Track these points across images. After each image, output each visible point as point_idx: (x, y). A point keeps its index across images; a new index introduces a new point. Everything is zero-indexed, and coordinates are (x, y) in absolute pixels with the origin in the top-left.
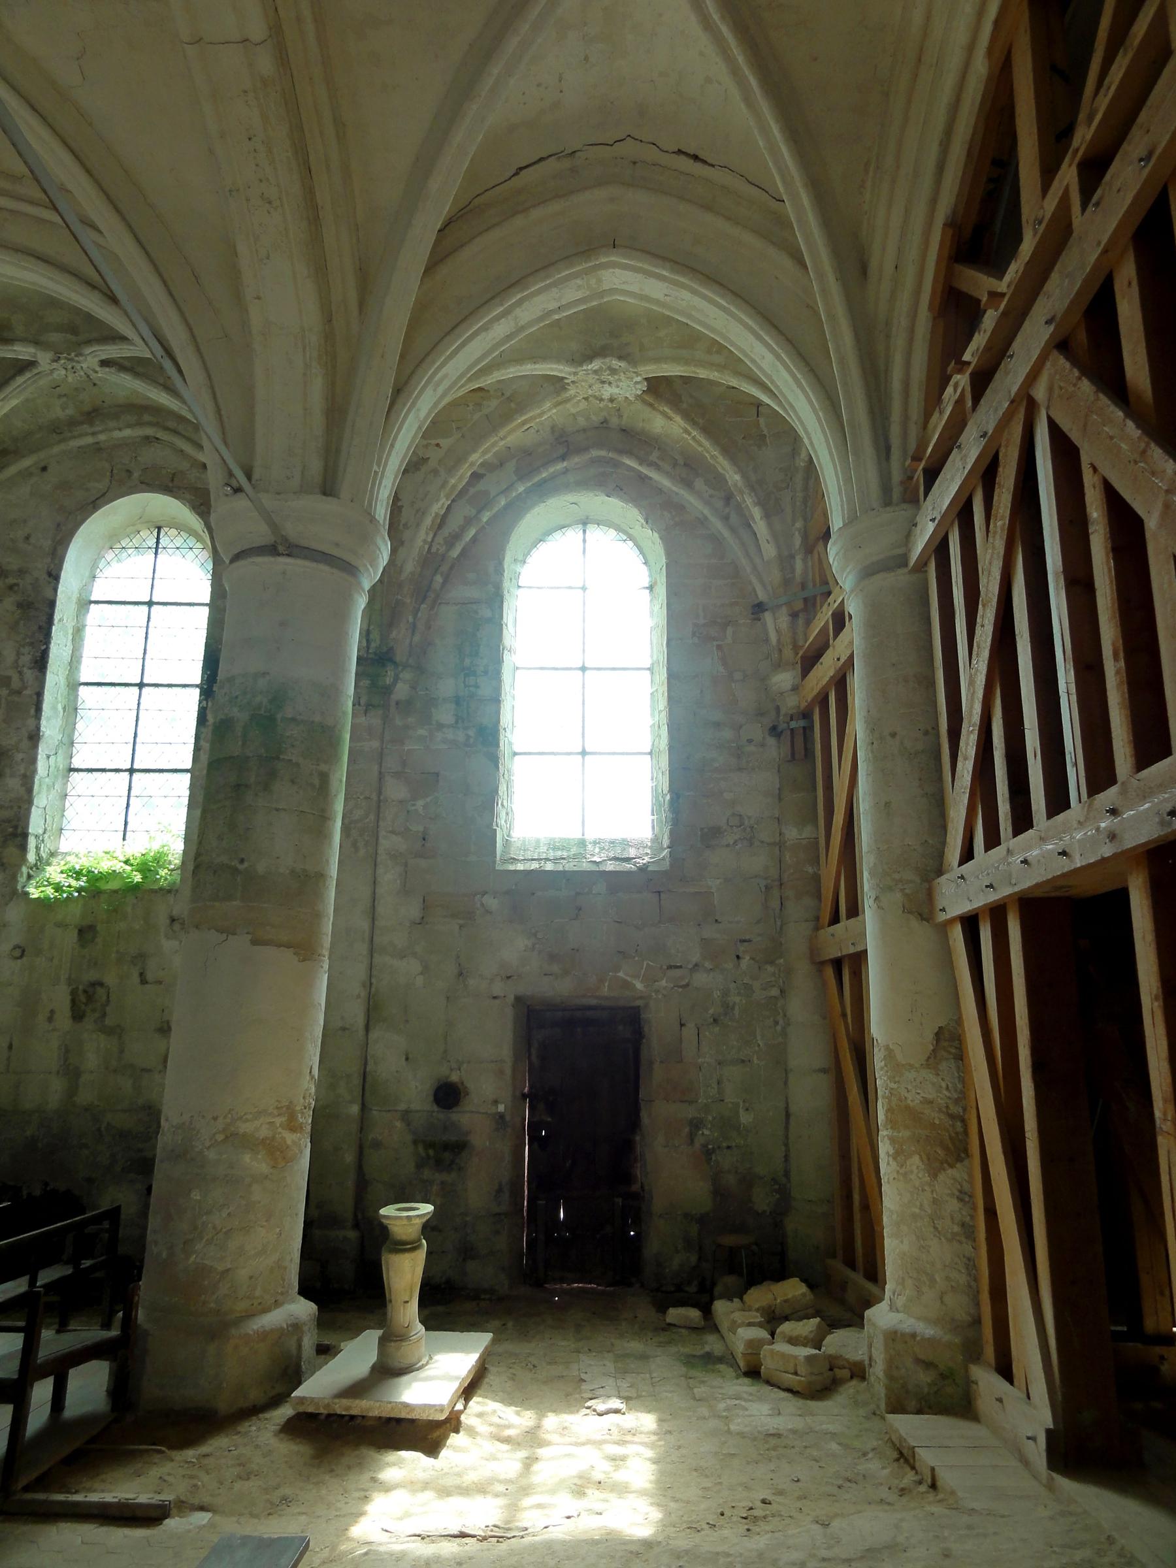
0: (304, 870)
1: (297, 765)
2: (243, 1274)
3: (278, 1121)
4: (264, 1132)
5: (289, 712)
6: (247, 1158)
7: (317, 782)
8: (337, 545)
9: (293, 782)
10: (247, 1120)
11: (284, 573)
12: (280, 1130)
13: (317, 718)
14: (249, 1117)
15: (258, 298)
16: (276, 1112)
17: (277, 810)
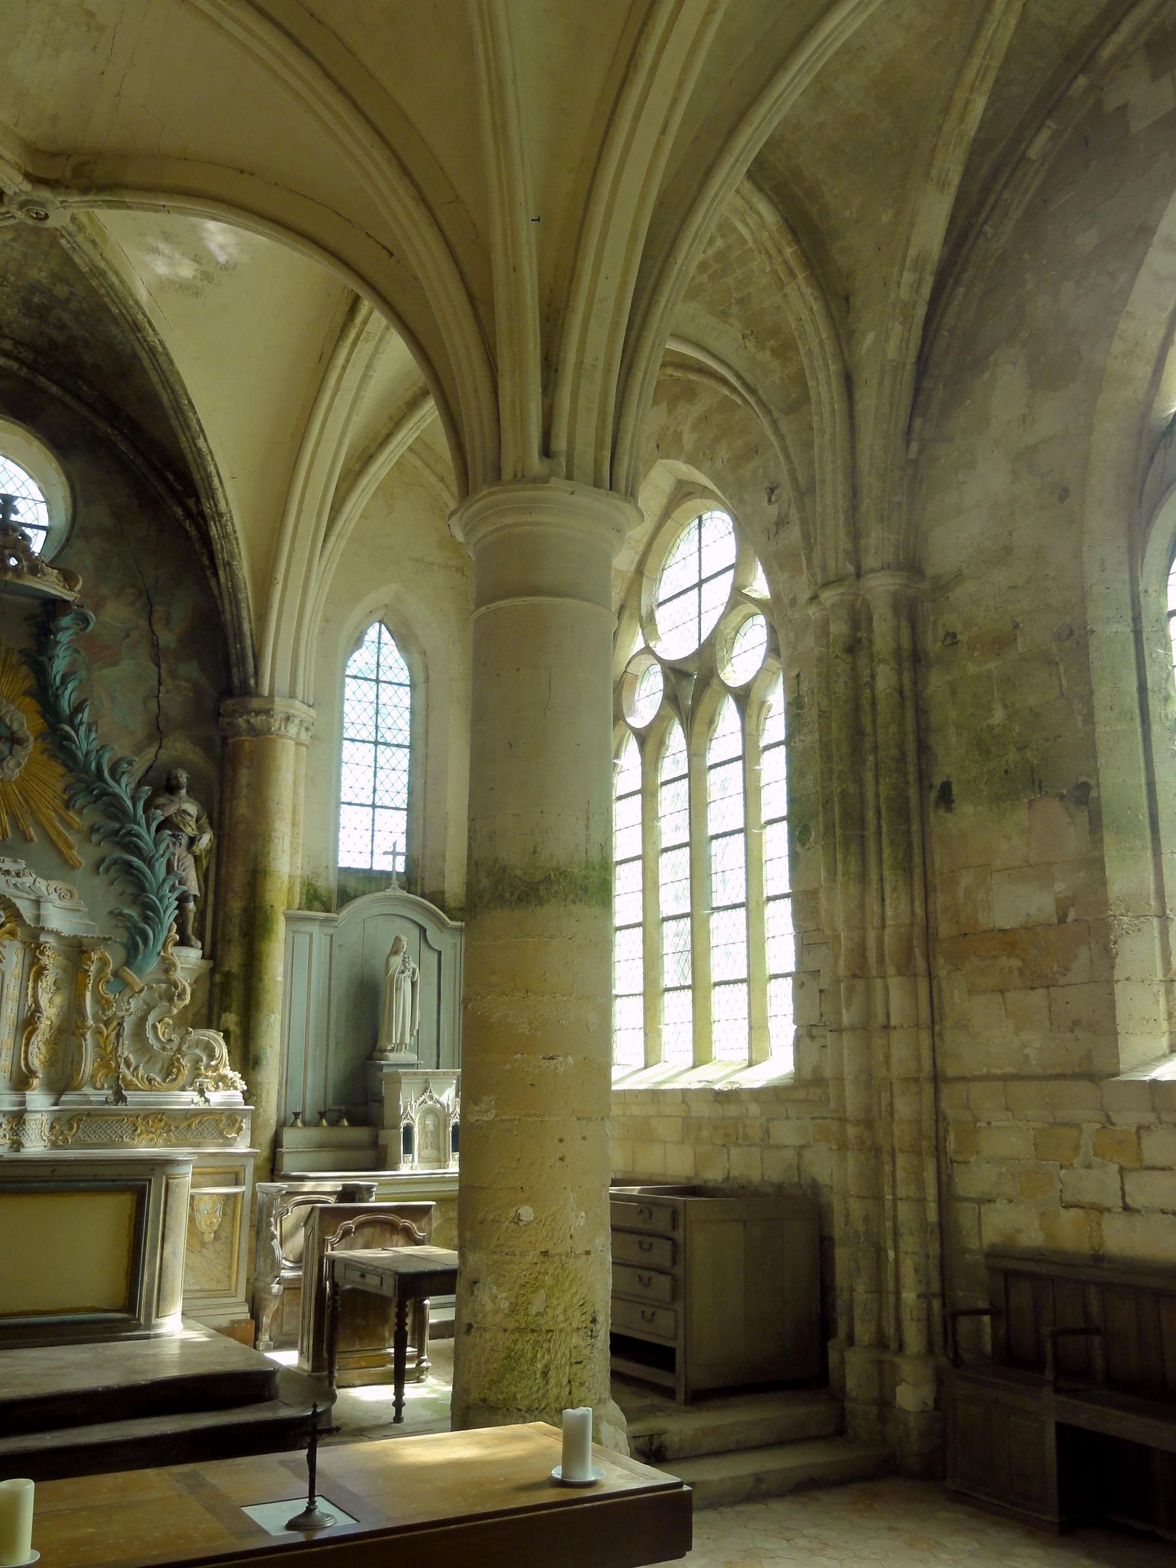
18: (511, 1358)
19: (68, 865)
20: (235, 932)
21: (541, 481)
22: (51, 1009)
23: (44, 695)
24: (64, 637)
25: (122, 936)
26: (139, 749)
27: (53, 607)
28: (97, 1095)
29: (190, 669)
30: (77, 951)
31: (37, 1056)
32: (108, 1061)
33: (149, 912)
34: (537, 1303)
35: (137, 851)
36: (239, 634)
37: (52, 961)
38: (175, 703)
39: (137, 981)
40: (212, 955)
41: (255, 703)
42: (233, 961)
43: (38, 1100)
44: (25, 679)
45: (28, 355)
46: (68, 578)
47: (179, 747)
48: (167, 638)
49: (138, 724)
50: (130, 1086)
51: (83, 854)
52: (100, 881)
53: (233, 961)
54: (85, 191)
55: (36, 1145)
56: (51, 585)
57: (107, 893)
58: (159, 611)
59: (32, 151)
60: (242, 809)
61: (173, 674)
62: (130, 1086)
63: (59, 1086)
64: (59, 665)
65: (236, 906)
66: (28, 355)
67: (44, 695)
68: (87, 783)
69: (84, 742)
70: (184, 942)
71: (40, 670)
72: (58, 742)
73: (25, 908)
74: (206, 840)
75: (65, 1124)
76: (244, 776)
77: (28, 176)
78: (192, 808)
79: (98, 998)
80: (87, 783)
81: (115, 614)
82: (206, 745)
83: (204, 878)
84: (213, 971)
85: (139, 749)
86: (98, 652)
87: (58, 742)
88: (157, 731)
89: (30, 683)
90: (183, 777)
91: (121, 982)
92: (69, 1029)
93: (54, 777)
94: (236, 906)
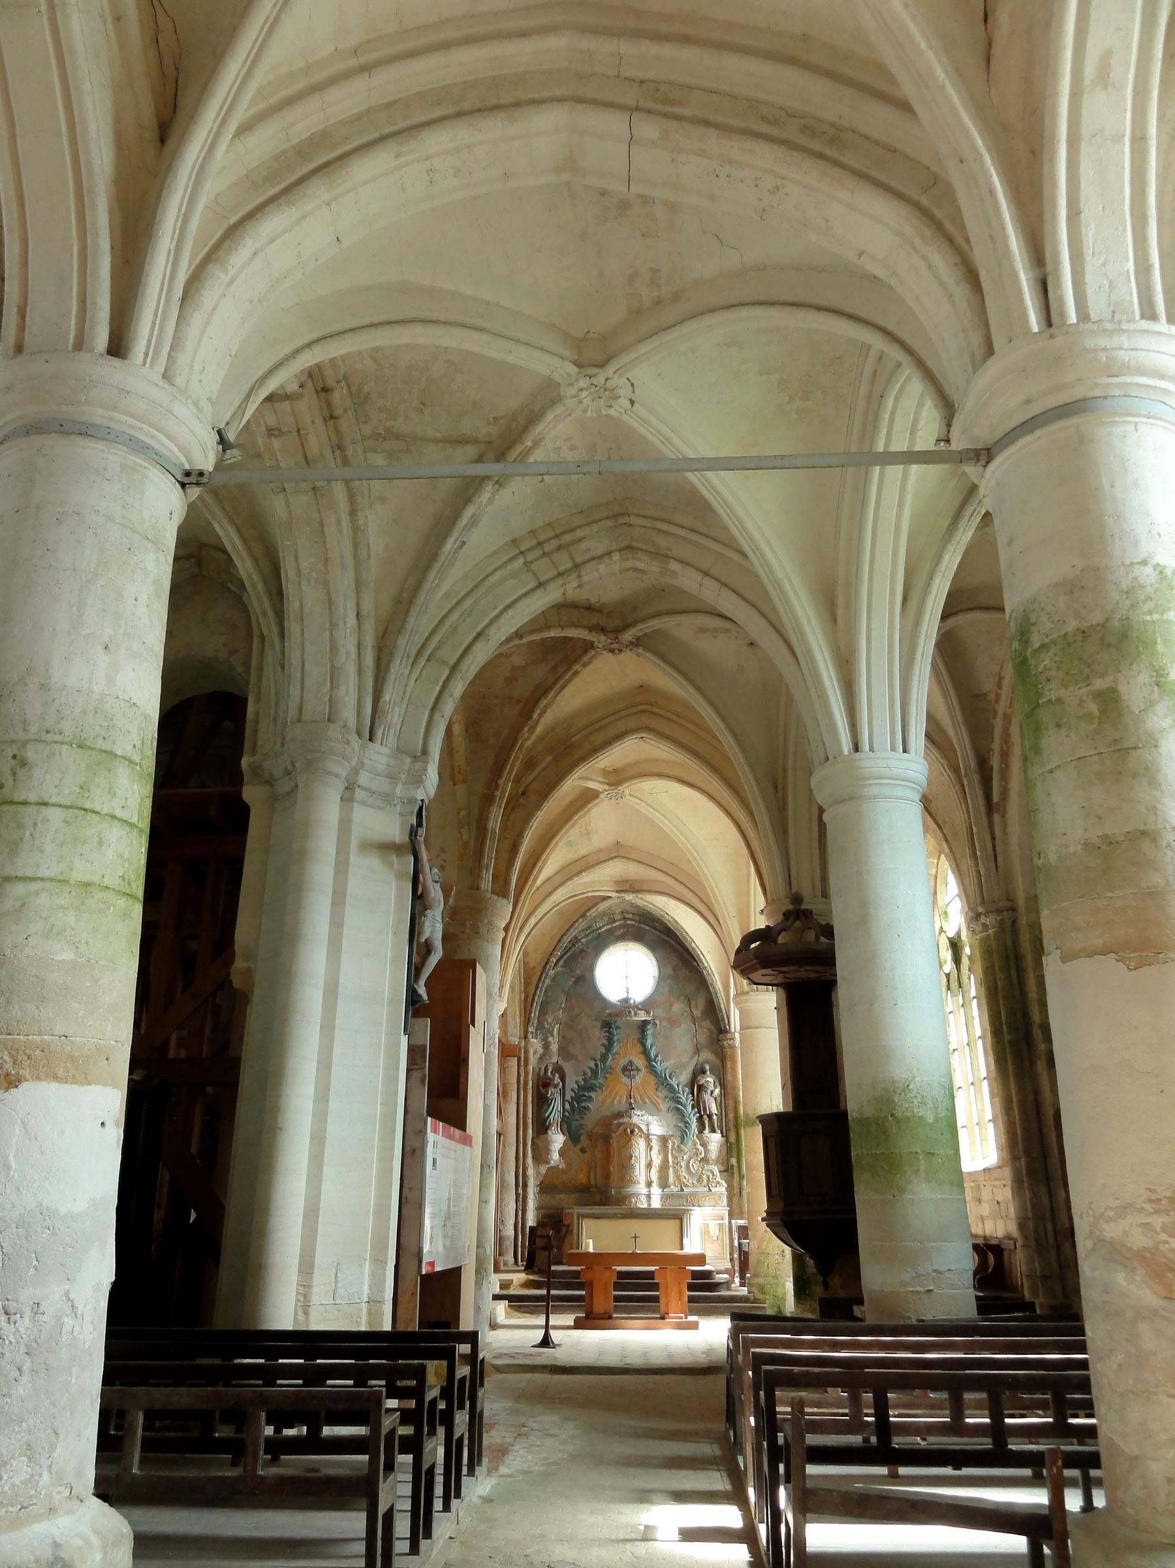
0: (1106, 836)
1: (1059, 701)
2: (1157, 1469)
3: (1158, 1221)
4: (1139, 1240)
5: (1036, 641)
6: (1120, 1278)
7: (1093, 707)
8: (1028, 401)
9: (1059, 726)
10: (1111, 1219)
11: (998, 483)
12: (1164, 1237)
13: (1071, 626)
14: (1112, 1213)
15: (860, 255)
16: (1148, 1206)
17: (1051, 771)
18: (759, 1262)
19: (659, 1110)
20: (731, 1126)
21: (748, 993)
22: (657, 1160)
23: (645, 1053)
24: (649, 1032)
25: (679, 1133)
26: (692, 1058)
27: (645, 1023)
28: (674, 1189)
29: (707, 1024)
30: (664, 1140)
31: (654, 1175)
32: (678, 1177)
33: (687, 1124)
34: (764, 1246)
35: (681, 1103)
36: (721, 1011)
37: (655, 1144)
38: (702, 1038)
39: (686, 1150)
40: (725, 1136)
41: (729, 1036)
42: (732, 1138)
43: (656, 1191)
44: (639, 1048)
45: (637, 918)
46: (648, 1013)
47: (706, 1055)
48: (697, 1013)
49: (690, 1048)
50: (686, 1186)
51: (663, 1106)
52: (670, 1115)
53: (732, 1138)
54: (633, 892)
55: (656, 1204)
56: (642, 1016)
57: (672, 1118)
58: (693, 1003)
59: (618, 882)
60: (729, 1077)
61: (701, 1027)
62: (686, 1186)
63: (664, 1184)
64: (649, 1043)
65: (731, 1116)
66: (637, 918)
67: (645, 1053)
68: (663, 1082)
69: (659, 1067)
70: (713, 1131)
71: (643, 1044)
72: (652, 1069)
73: (643, 1127)
74: (717, 1091)
75: (665, 1198)
76: (729, 1064)
77: (617, 892)
78: (711, 1079)
79: (673, 1156)
80: (663, 1082)
81: (678, 1007)
82: (716, 1053)
83: (719, 1106)
84: (727, 1141)
85: (692, 1058)
86: (673, 1022)
87: (652, 1069)
88: (697, 1051)
89: (641, 1049)
90: (707, 1067)
91: (680, 1150)
92: (664, 1167)
93: (652, 1080)
94: (731, 1116)
